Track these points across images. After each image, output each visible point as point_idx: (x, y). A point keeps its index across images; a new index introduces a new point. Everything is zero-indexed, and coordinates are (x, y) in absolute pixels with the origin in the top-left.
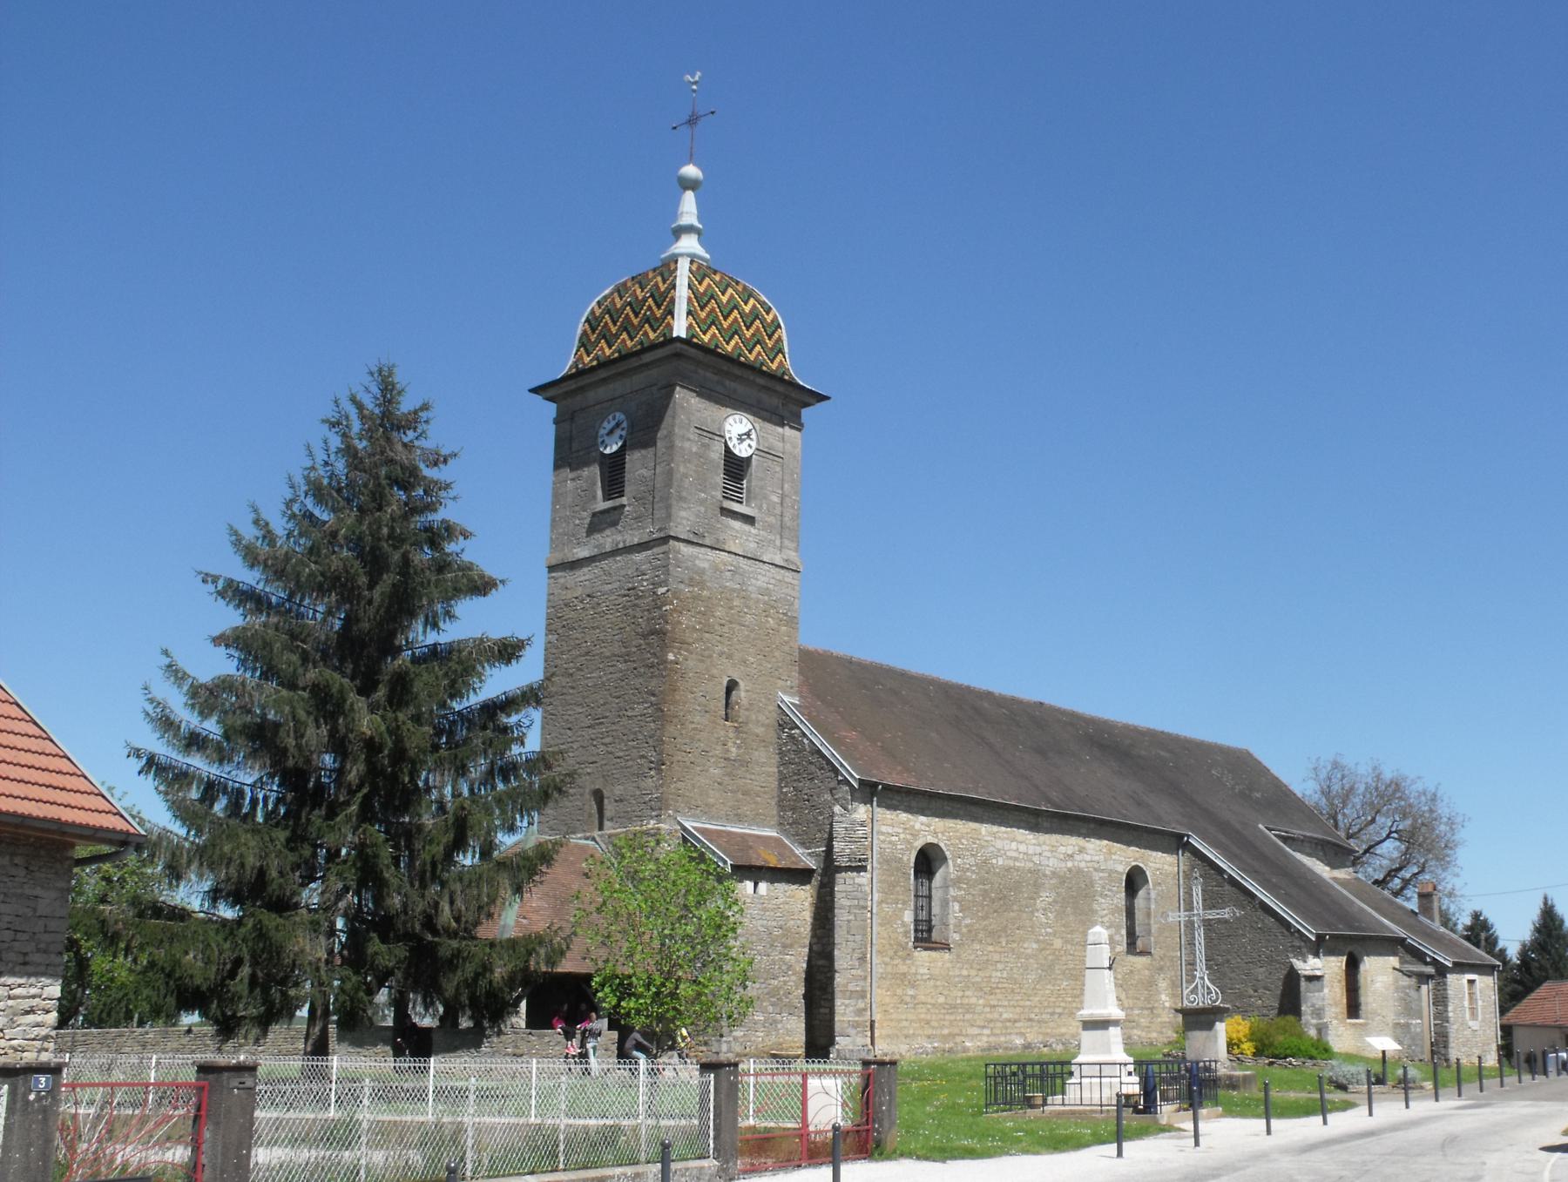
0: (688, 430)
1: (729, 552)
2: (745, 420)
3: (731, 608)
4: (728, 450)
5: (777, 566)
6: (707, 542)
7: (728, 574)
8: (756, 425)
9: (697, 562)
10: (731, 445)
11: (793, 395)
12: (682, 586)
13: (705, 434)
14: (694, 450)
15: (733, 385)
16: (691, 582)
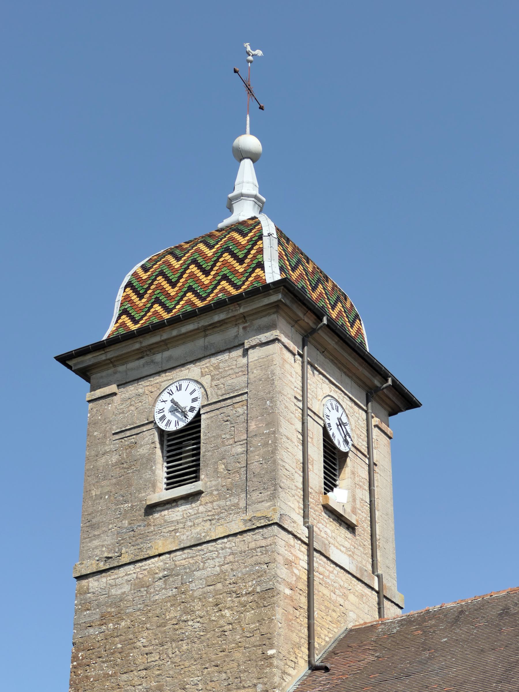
0: (104, 443)
1: (160, 555)
2: (184, 384)
3: (164, 625)
4: (162, 433)
5: (235, 535)
6: (125, 559)
7: (160, 583)
8: (206, 381)
9: (113, 591)
10: (162, 426)
11: (242, 310)
12: (91, 630)
13: (128, 433)
14: (115, 459)
15: (166, 354)
16: (104, 619)
